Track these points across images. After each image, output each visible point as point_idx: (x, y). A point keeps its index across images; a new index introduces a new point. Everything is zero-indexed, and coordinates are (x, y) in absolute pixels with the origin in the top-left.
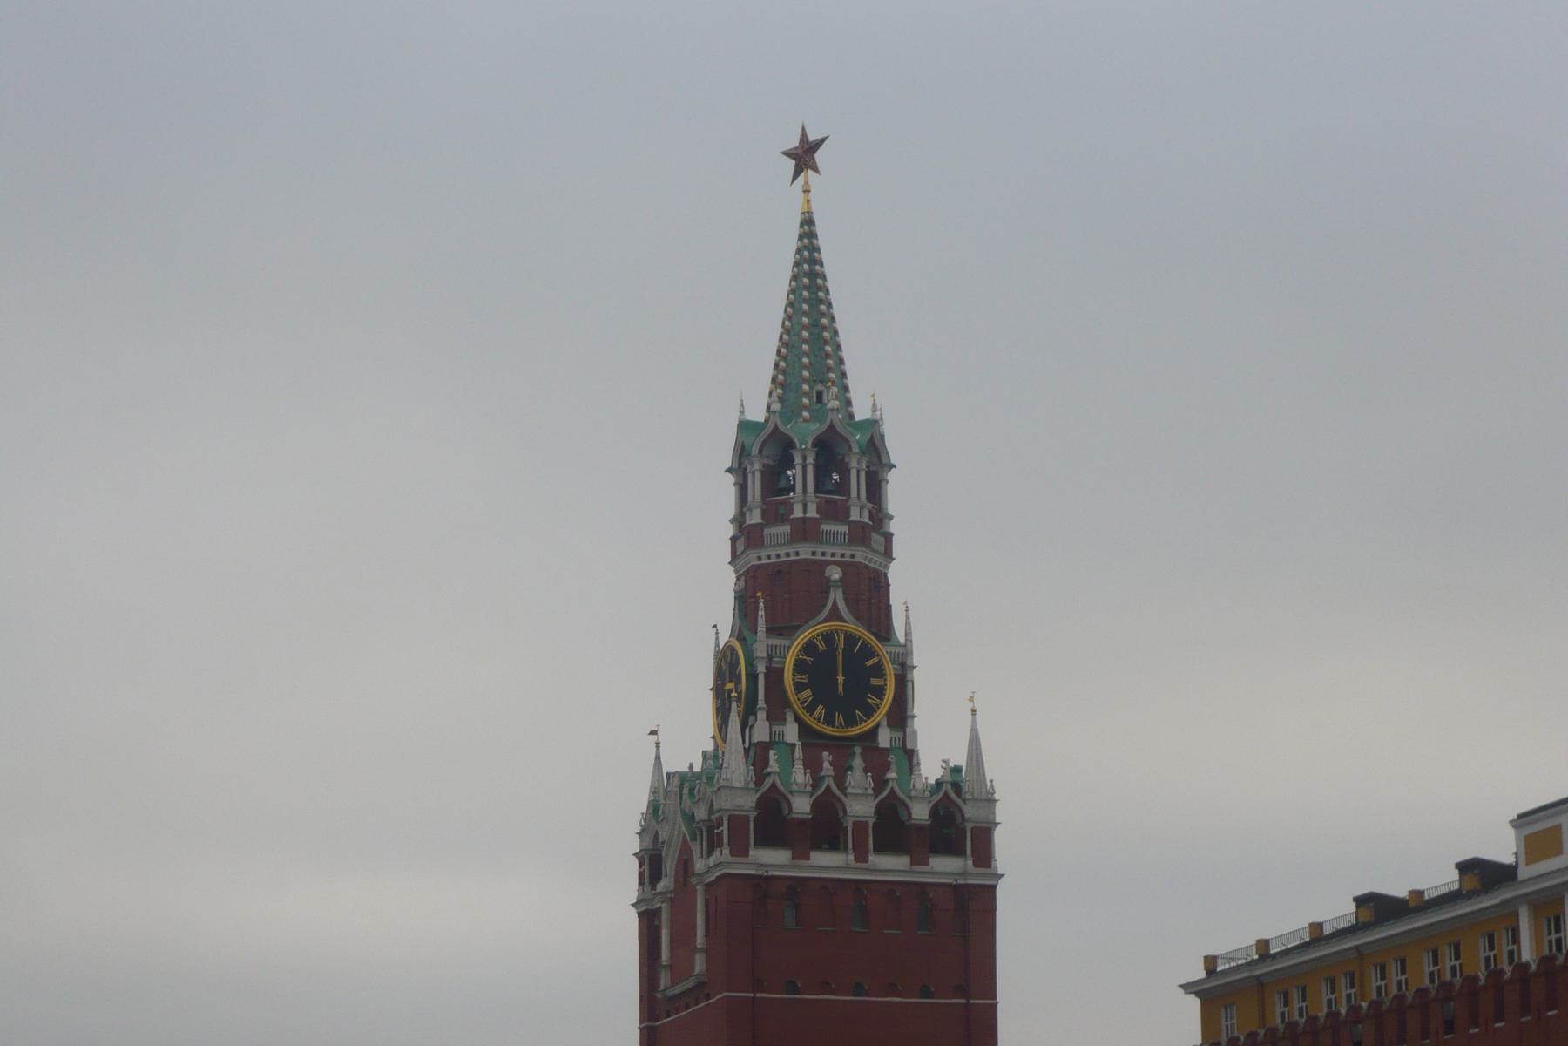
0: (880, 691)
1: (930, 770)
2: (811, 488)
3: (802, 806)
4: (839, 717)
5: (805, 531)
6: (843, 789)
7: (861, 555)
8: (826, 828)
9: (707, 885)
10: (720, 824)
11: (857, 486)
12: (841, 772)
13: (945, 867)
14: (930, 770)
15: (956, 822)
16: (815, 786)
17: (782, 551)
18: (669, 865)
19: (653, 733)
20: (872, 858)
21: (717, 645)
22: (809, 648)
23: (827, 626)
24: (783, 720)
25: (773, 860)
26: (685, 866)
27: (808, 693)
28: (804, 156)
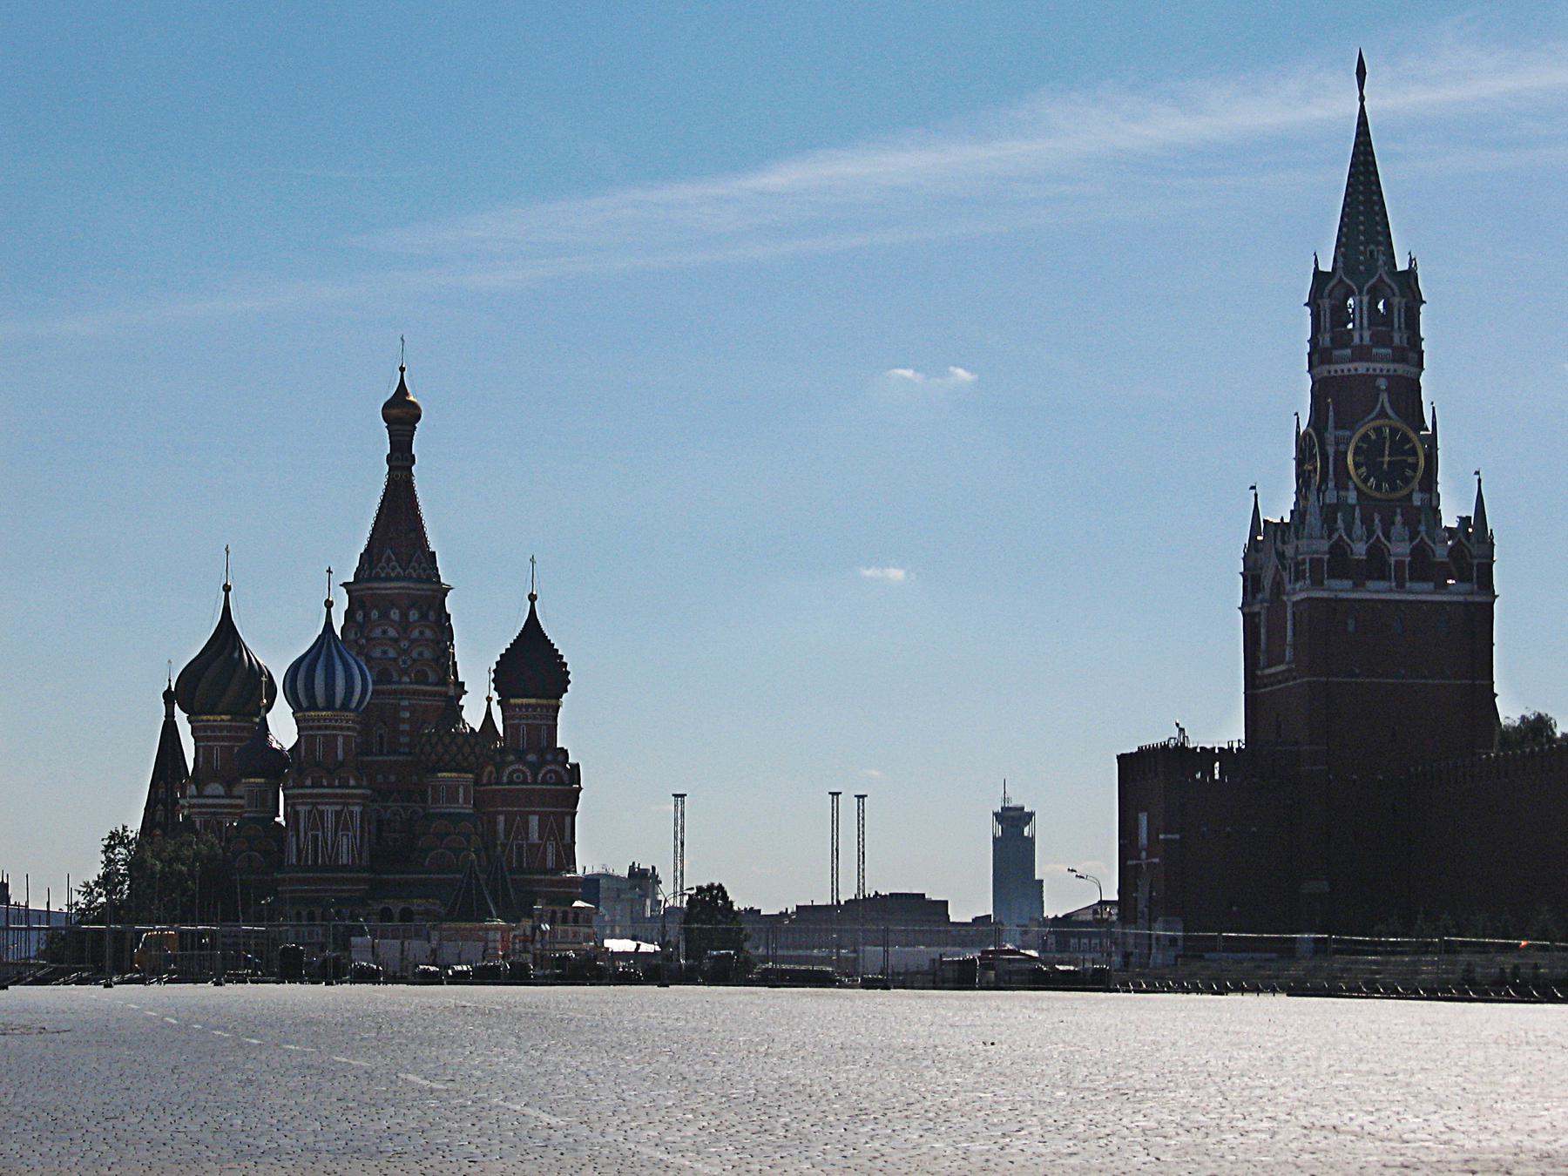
0: (1414, 467)
1: (1449, 520)
2: (1366, 314)
3: (1360, 549)
4: (1385, 486)
6: (1388, 538)
7: (1401, 369)
8: (1376, 565)
9: (1295, 604)
10: (1304, 562)
12: (1387, 525)
14: (1449, 520)
16: (1369, 538)
17: (1345, 367)
18: (1267, 582)
19: (1253, 488)
20: (1408, 584)
21: (1298, 433)
22: (1365, 437)
23: (1378, 423)
24: (1347, 489)
25: (1341, 589)
26: (1278, 586)
27: (1364, 469)
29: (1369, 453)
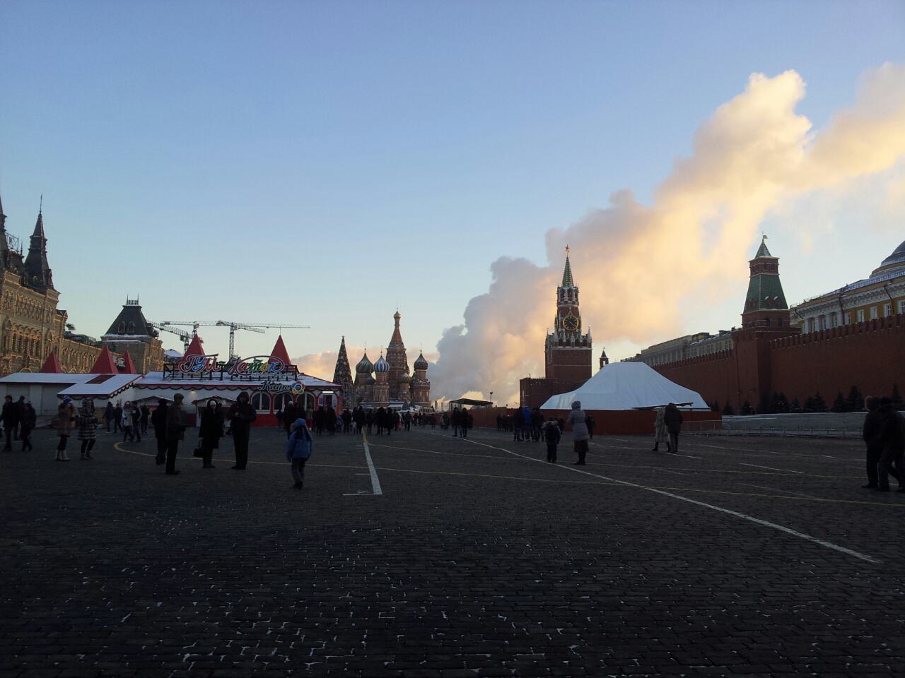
1: (583, 334)
3: (565, 341)
5: (566, 303)
7: (575, 306)
8: (568, 343)
11: (574, 296)
13: (584, 348)
14: (583, 334)
15: (587, 342)
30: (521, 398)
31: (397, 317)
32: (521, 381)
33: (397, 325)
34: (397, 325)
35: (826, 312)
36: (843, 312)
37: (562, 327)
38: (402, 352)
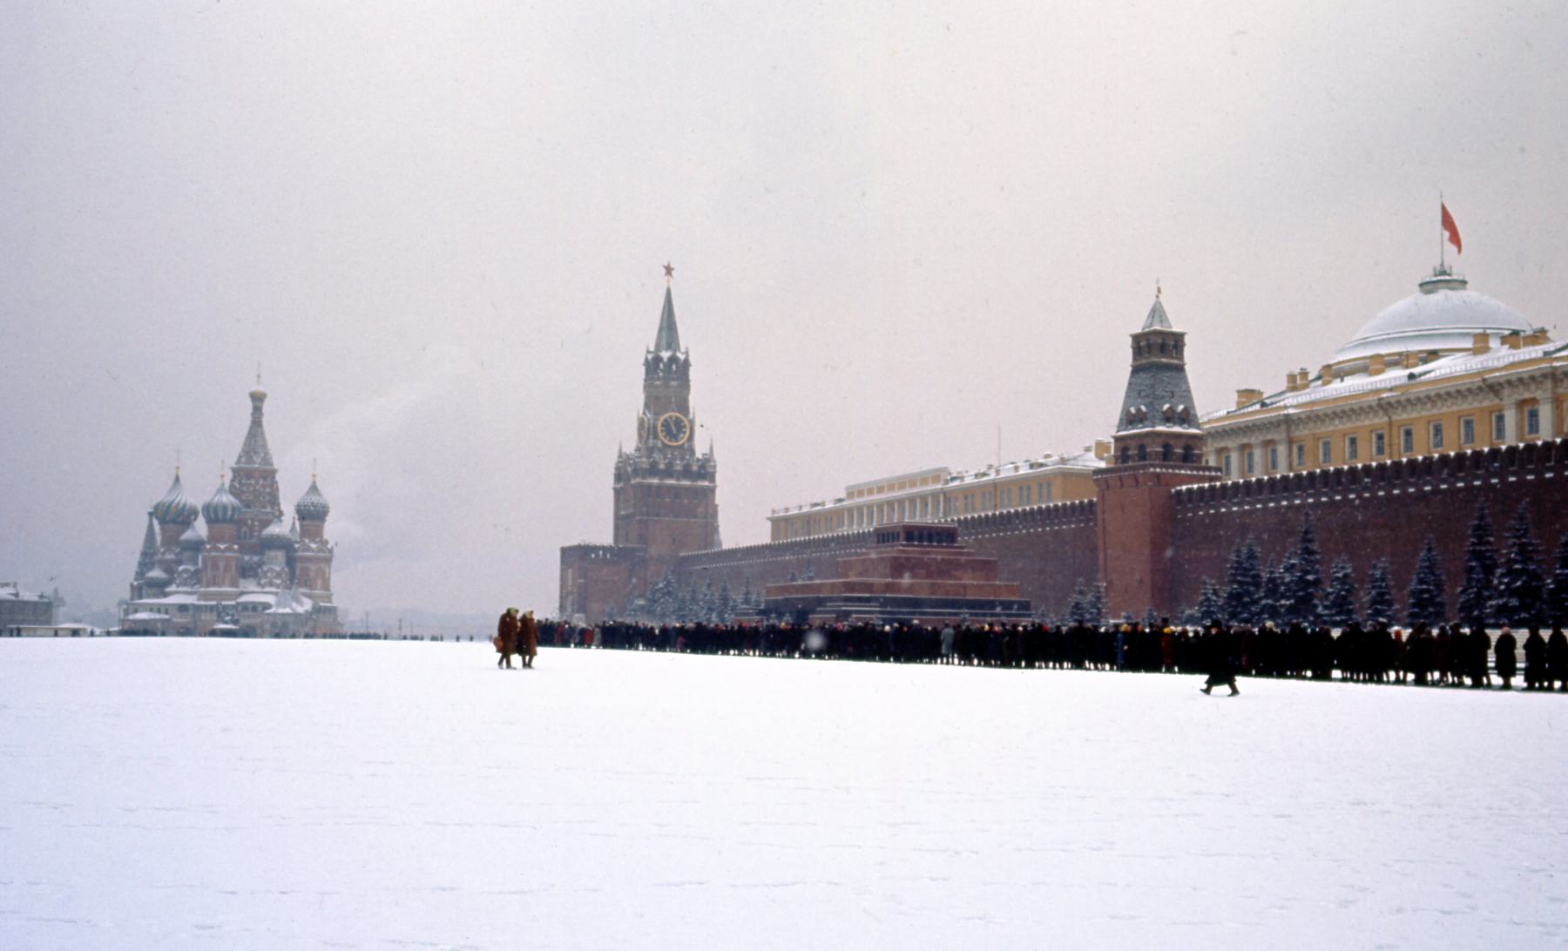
3: (662, 466)
8: (669, 473)
14: (699, 455)
15: (705, 470)
28: (669, 270)
29: (666, 425)
30: (562, 587)
31: (258, 399)
32: (565, 552)
33: (257, 411)
34: (257, 411)
35: (1255, 439)
36: (1290, 442)
37: (656, 437)
38: (269, 475)
